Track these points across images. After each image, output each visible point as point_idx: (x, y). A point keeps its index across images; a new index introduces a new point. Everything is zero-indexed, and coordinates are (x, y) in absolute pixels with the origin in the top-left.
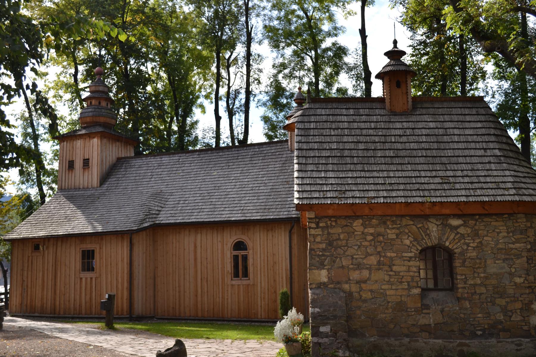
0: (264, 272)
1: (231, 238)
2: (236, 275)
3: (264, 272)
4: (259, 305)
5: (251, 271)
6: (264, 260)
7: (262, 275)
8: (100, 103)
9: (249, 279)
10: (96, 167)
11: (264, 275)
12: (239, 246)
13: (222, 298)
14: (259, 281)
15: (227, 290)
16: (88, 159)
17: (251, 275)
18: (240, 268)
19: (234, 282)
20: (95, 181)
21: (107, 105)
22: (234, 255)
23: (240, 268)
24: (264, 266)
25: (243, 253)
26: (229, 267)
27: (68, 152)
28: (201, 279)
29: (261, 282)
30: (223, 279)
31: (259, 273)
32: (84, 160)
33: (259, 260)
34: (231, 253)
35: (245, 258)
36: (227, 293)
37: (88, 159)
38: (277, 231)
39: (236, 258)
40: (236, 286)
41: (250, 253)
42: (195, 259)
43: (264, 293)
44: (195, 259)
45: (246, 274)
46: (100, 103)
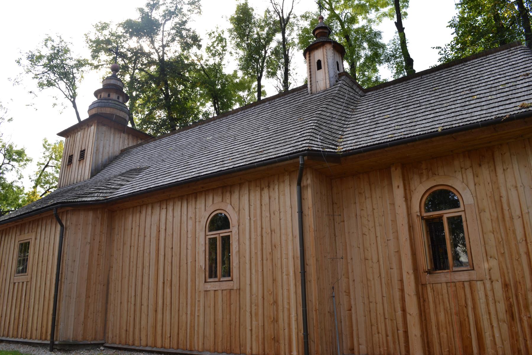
0: (256, 264)
1: (204, 209)
2: (212, 273)
3: (256, 264)
4: (249, 328)
5: (234, 264)
6: (256, 242)
7: (253, 271)
8: (109, 95)
9: (232, 280)
10: (89, 157)
11: (257, 271)
12: (220, 222)
13: (191, 314)
14: (248, 282)
15: (199, 301)
16: (84, 150)
17: (235, 272)
18: (219, 259)
19: (209, 286)
20: (87, 174)
21: (118, 98)
22: (210, 239)
23: (219, 259)
24: (256, 253)
25: (223, 233)
26: (202, 261)
27: (70, 147)
28: (164, 283)
29: (251, 285)
30: (194, 281)
31: (248, 266)
32: (81, 151)
33: (247, 243)
34: (206, 235)
35: (226, 240)
36: (199, 306)
37: (84, 150)
38: (276, 187)
39: (213, 242)
40: (212, 293)
41: (233, 231)
42: (158, 250)
43: (257, 305)
44: (158, 250)
45: (228, 273)
46: (109, 95)
